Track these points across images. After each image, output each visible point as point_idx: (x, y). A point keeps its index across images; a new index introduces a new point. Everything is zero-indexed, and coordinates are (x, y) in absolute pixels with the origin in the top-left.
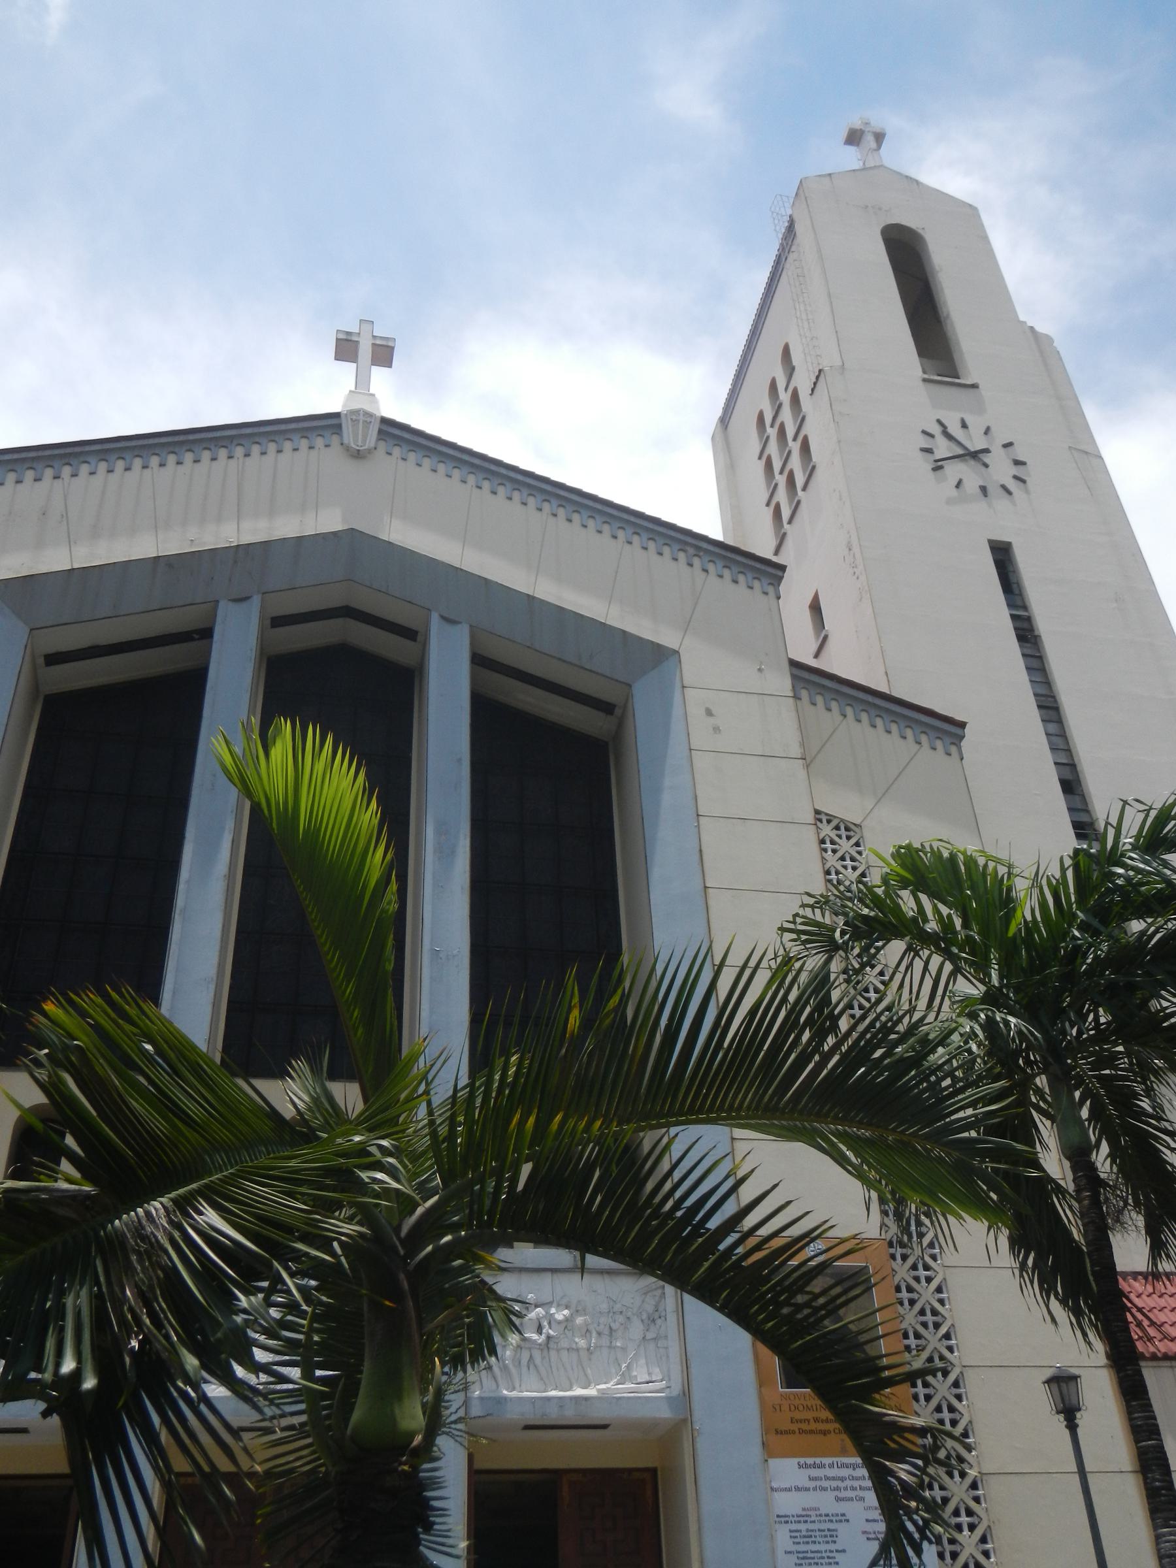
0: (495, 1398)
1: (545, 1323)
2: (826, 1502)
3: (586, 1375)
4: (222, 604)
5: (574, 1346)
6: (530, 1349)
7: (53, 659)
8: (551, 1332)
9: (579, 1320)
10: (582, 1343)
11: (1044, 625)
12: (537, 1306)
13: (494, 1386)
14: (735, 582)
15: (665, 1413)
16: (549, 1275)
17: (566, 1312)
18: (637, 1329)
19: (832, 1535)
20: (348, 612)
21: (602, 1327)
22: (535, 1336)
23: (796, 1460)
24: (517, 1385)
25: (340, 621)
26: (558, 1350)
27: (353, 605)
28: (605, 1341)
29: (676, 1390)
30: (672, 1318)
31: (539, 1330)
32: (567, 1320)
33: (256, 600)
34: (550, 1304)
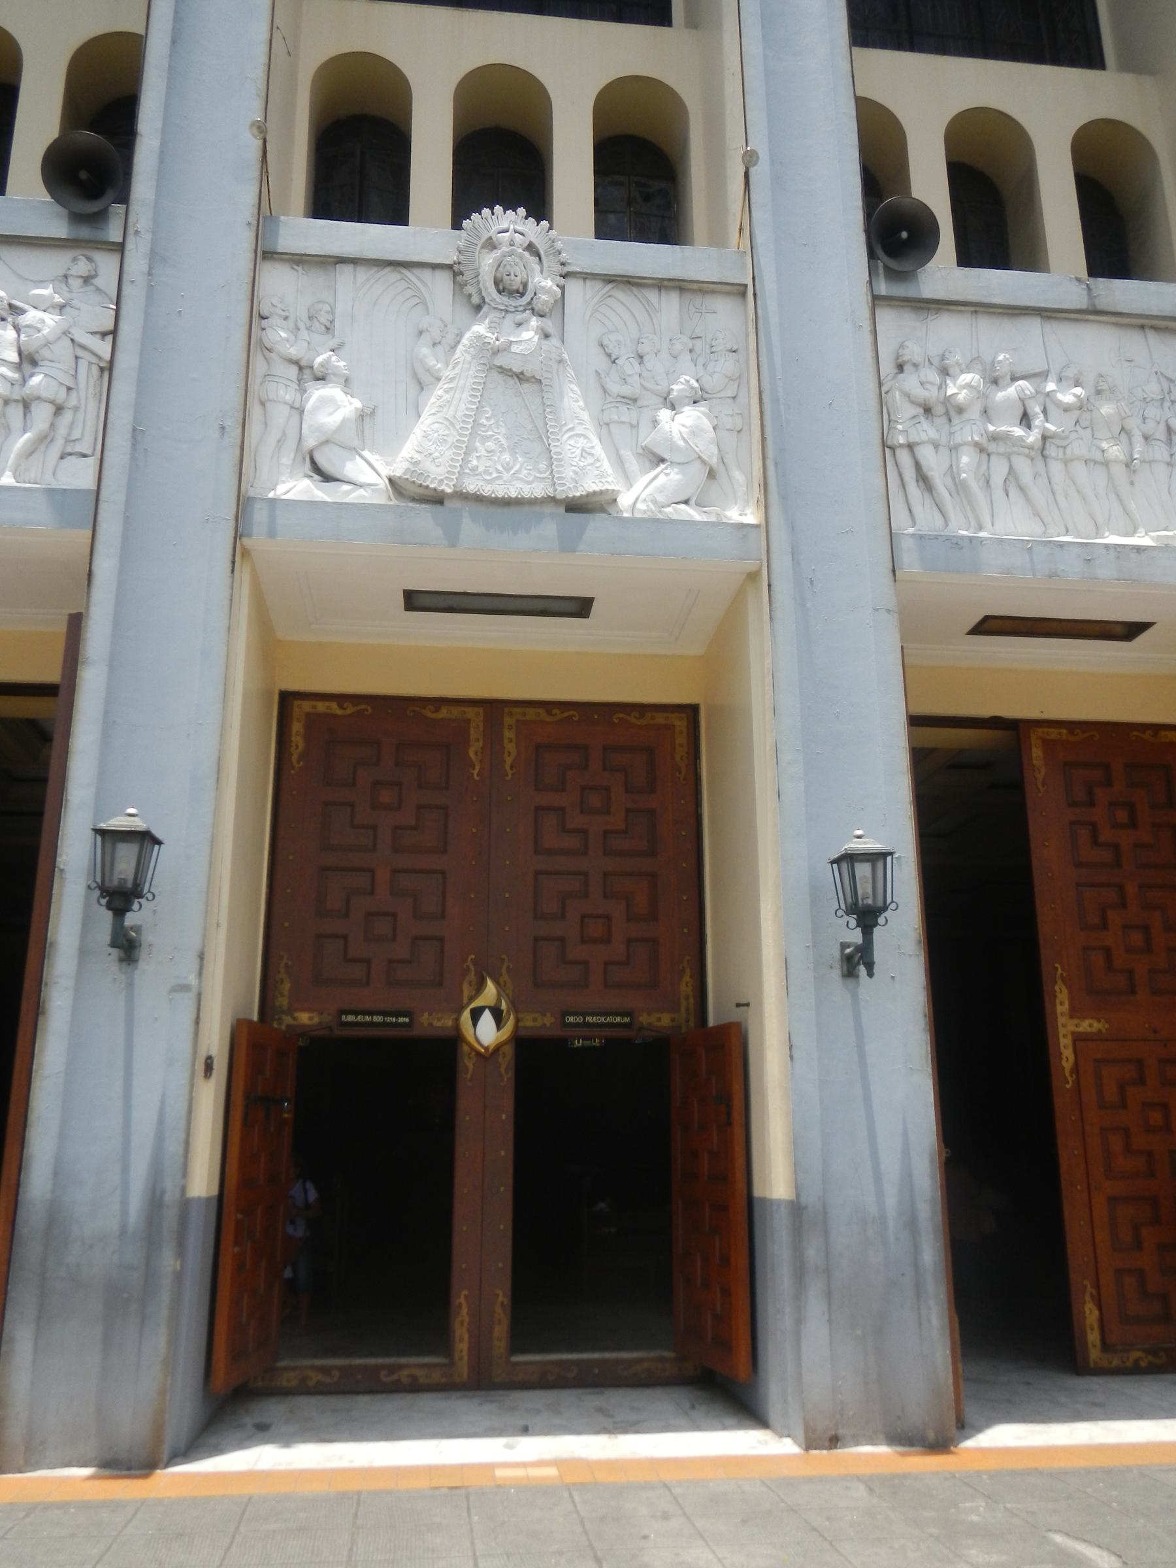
0: (948, 539)
1: (1038, 409)
3: (1127, 512)
5: (1098, 456)
6: (1008, 456)
8: (1048, 425)
9: (1107, 409)
10: (1115, 451)
12: (1014, 379)
13: (939, 521)
16: (1034, 325)
17: (1078, 391)
21: (1151, 424)
22: (1018, 431)
24: (987, 521)
26: (1066, 462)
31: (1025, 419)
32: (1081, 406)
34: (1044, 375)
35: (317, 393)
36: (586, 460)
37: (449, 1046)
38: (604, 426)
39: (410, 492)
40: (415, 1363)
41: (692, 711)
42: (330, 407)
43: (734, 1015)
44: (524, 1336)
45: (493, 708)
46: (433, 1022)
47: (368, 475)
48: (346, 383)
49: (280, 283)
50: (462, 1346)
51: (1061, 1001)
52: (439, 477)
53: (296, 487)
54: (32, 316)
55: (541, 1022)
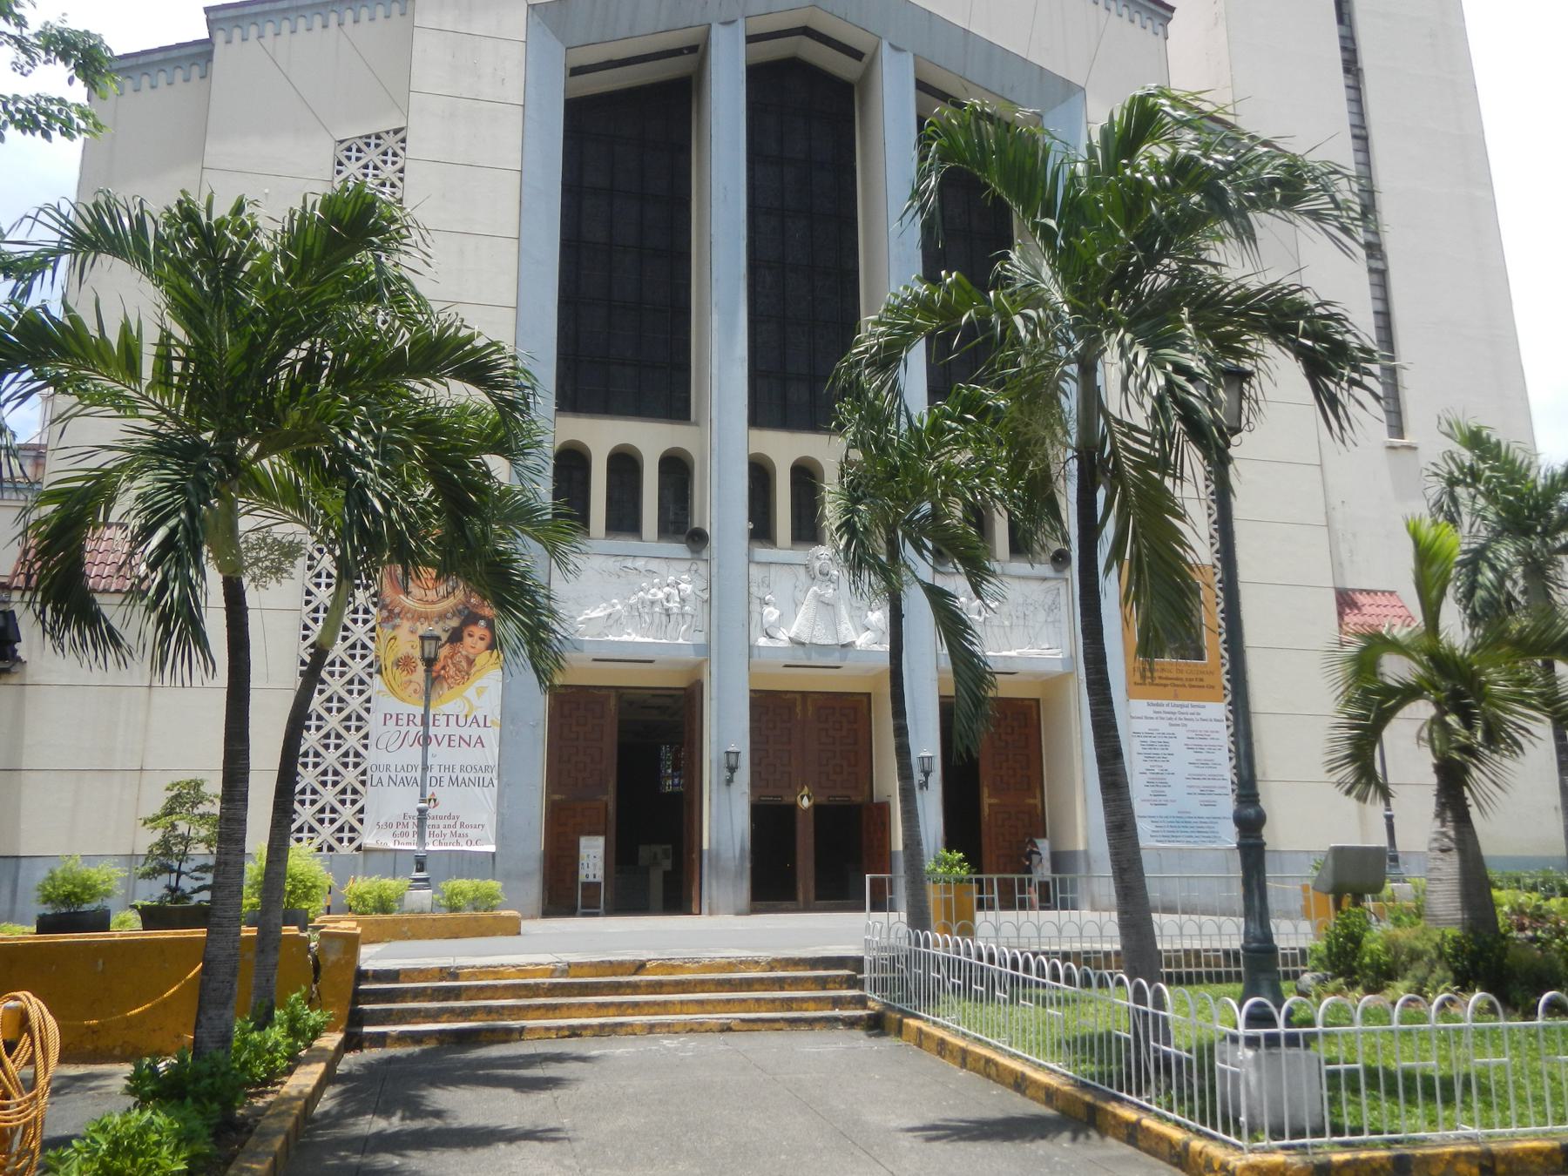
2: (1164, 726)
4: (714, 26)
7: (575, 72)
11: (1366, 60)
14: (1132, 21)
15: (1059, 669)
18: (1042, 616)
19: (1166, 745)
20: (806, 31)
23: (1145, 702)
25: (795, 39)
27: (812, 26)
28: (1021, 622)
29: (1067, 655)
30: (1064, 609)
33: (741, 23)
35: (767, 610)
36: (847, 632)
37: (793, 807)
38: (851, 617)
39: (797, 643)
40: (786, 904)
41: (869, 695)
42: (771, 613)
43: (883, 799)
44: (818, 897)
45: (804, 694)
46: (788, 800)
47: (783, 637)
48: (775, 606)
49: (754, 569)
50: (801, 896)
51: (985, 792)
52: (805, 638)
53: (762, 641)
54: (682, 586)
55: (822, 800)
